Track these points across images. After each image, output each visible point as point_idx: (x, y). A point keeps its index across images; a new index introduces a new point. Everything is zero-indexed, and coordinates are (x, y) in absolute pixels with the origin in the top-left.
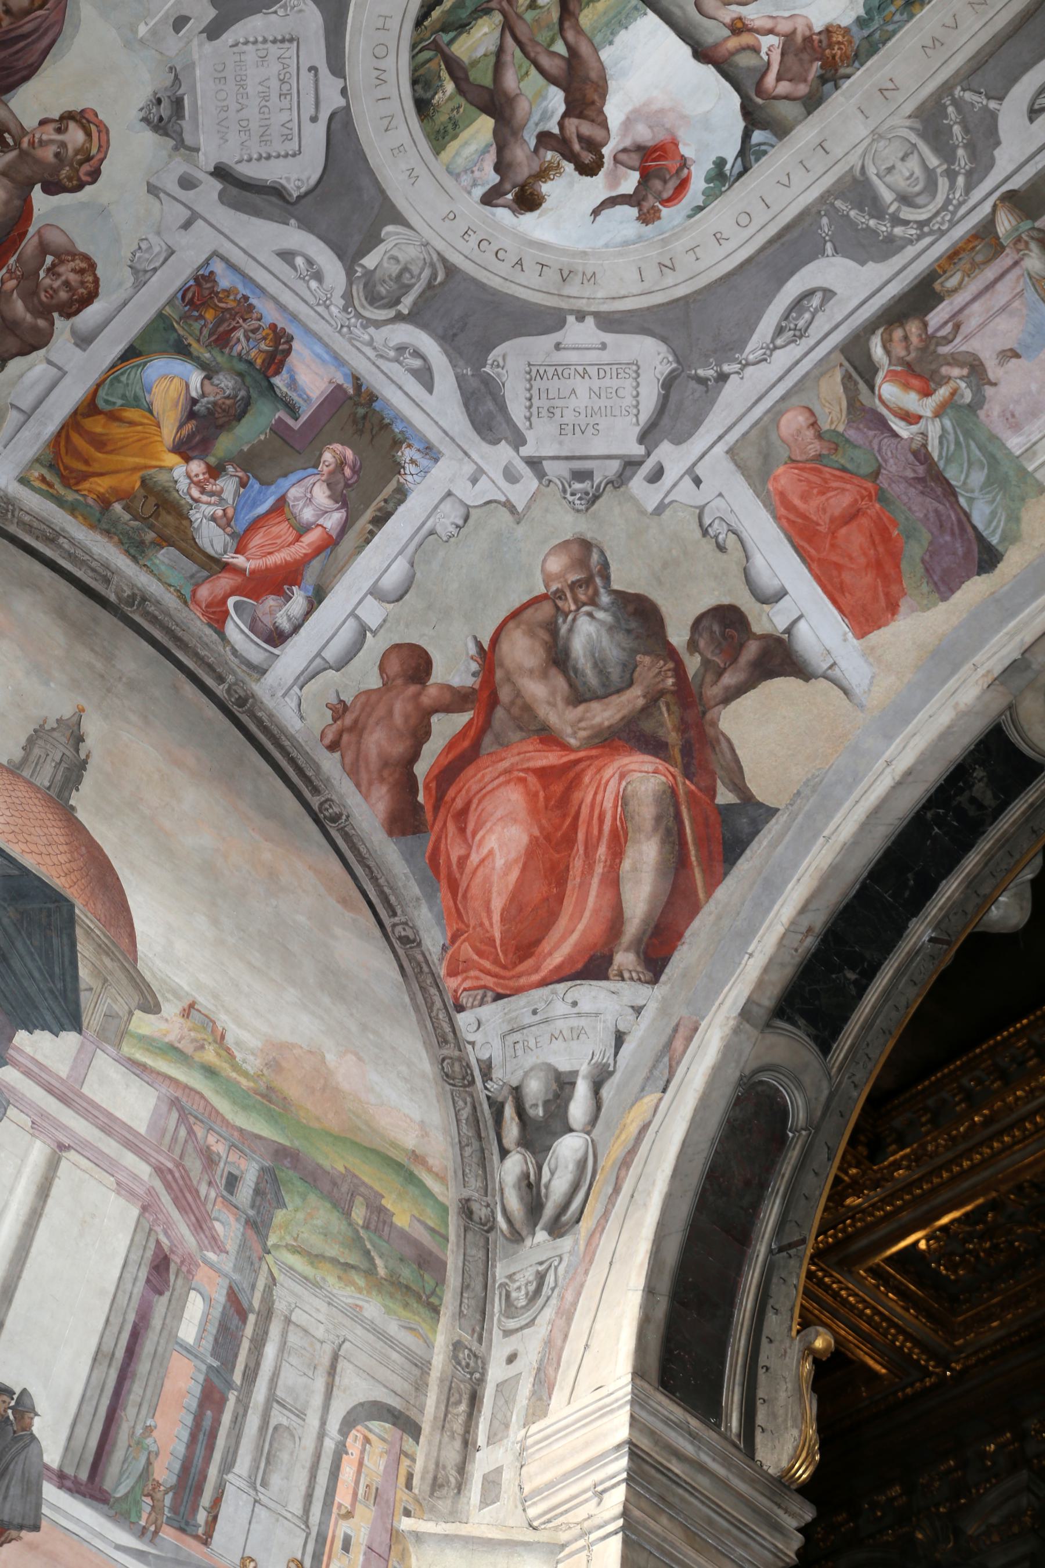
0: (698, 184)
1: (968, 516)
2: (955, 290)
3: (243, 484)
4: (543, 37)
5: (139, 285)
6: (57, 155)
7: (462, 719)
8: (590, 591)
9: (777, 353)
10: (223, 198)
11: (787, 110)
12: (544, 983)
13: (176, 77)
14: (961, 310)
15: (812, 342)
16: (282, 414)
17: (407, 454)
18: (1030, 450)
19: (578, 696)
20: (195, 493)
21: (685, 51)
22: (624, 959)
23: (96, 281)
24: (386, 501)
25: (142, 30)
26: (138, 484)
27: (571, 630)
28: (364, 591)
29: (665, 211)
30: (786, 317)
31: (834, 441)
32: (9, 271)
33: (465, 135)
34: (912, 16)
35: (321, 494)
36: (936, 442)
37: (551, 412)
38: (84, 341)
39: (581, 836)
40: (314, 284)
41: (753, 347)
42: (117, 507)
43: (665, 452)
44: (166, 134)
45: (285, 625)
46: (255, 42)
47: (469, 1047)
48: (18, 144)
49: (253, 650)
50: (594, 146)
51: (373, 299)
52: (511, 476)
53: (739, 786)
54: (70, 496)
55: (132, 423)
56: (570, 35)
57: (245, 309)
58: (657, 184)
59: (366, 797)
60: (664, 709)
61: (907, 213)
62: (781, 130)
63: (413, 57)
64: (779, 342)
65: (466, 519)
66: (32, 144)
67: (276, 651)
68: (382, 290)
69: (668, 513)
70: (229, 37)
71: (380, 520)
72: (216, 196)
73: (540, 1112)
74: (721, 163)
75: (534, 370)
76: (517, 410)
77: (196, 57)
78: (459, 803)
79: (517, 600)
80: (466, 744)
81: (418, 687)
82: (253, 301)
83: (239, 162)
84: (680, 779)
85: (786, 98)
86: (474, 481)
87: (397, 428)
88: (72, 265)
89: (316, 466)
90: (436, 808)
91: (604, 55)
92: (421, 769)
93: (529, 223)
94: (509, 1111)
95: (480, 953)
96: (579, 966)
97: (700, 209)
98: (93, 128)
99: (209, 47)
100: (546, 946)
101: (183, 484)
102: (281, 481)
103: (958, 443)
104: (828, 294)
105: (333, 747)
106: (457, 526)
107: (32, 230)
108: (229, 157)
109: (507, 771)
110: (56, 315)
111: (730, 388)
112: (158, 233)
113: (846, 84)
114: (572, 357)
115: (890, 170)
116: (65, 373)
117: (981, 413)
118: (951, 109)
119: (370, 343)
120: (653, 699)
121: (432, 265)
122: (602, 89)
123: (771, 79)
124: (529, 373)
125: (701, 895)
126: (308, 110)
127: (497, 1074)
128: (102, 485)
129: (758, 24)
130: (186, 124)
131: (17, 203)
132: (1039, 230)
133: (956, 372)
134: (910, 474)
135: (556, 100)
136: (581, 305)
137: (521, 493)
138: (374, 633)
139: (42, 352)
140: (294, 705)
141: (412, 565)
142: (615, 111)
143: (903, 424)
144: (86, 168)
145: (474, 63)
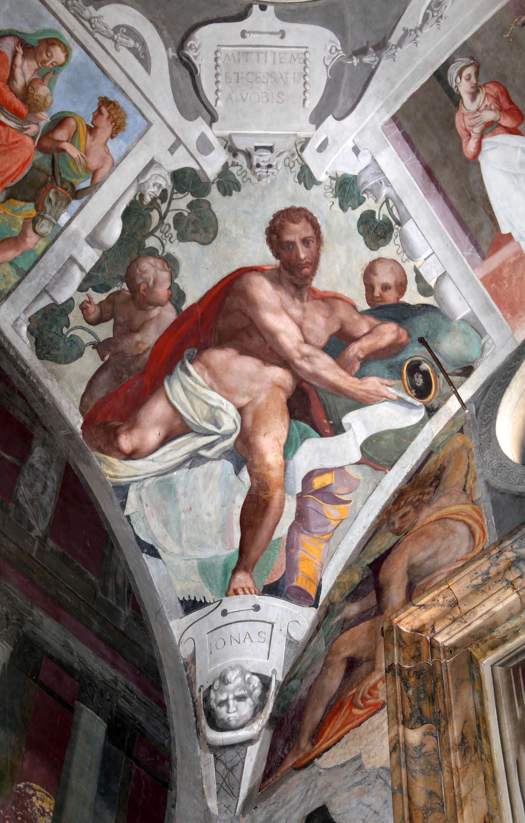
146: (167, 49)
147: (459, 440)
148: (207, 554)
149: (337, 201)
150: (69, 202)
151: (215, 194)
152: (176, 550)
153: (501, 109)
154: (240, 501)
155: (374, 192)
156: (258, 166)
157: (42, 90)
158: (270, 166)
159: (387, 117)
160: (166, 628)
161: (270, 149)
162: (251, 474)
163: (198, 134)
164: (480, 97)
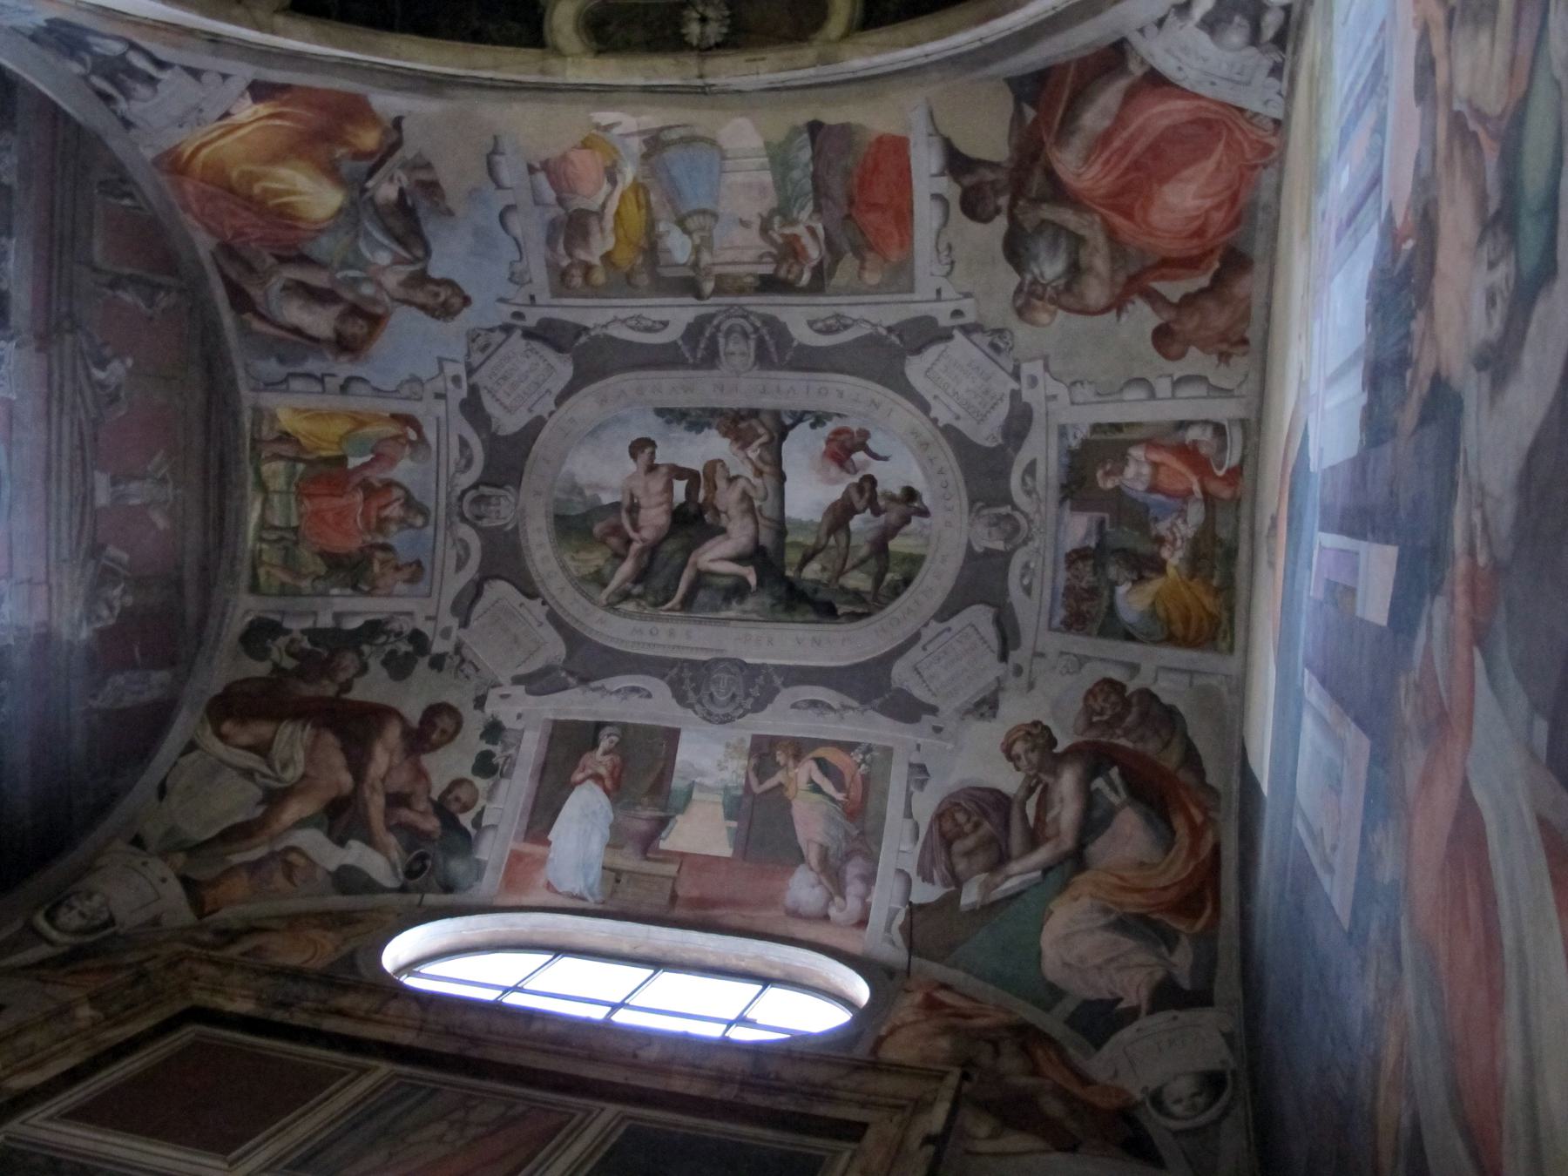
0: (831, 426)
1: (813, 158)
2: (750, 274)
3: (1156, 520)
4: (833, 553)
5: (1088, 658)
6: (1033, 750)
7: (1161, 286)
8: (1034, 287)
9: (855, 316)
10: (1017, 646)
11: (766, 418)
12: (1197, 96)
14: (755, 263)
15: (835, 308)
16: (1108, 528)
17: (1074, 444)
18: (762, 168)
19: (1078, 241)
20: (1179, 543)
21: (787, 485)
22: (1136, 70)
23: (1097, 684)
24: (1105, 433)
25: (950, 746)
26: (1196, 580)
27: (1059, 277)
28: (1159, 402)
29: (855, 429)
30: (837, 331)
31: (858, 252)
32: (1112, 736)
33: (907, 551)
34: (688, 409)
35: (1130, 471)
36: (806, 209)
37: (987, 392)
38: (1134, 668)
39: (1125, 163)
40: (1032, 565)
41: (865, 330)
42: (1215, 582)
43: (944, 321)
45: (1209, 431)
46: (927, 686)
47: (1284, 93)
48: (1036, 776)
49: (1235, 436)
50: (859, 487)
51: (1017, 529)
52: (1034, 381)
53: (1018, 114)
54: (1225, 615)
55: (1166, 610)
56: (823, 542)
57: (1069, 590)
58: (848, 444)
59: (1249, 297)
60: (1034, 191)
61: (749, 329)
62: (776, 414)
63: (887, 605)
64: (849, 322)
65: (1074, 383)
67: (1226, 423)
68: (1008, 528)
69: (965, 290)
70: (932, 701)
71: (1117, 427)
72: (1019, 652)
73: (1237, 19)
74: (813, 426)
75: (979, 418)
76: (1003, 409)
78: (1195, 242)
79: (1078, 322)
80: (1164, 271)
81: (1172, 325)
82: (1061, 590)
83: (993, 651)
84: (1048, 145)
85: (763, 425)
86: (1054, 397)
87: (1066, 460)
89: (1118, 489)
90: (1212, 251)
91: (818, 519)
92: (1204, 281)
93: (919, 484)
94: (1269, 32)
95: (1240, 144)
96: (1166, 89)
97: (839, 415)
98: (1011, 740)
99: (942, 707)
100: (1185, 117)
101: (1179, 554)
102: (1140, 500)
103: (796, 199)
104: (811, 324)
105: (1245, 342)
106: (1082, 383)
107: (1081, 739)
108: (991, 658)
109: (1151, 235)
110: (1127, 694)
111: (891, 320)
112: (1054, 668)
113: (735, 407)
114: (956, 408)
115: (743, 354)
117: (775, 205)
118: (699, 355)
119: (1038, 511)
120: (1038, 201)
121: (979, 510)
122: (833, 507)
123: (764, 439)
124: (982, 420)
125: (1072, 69)
126: (947, 635)
127: (1267, 63)
128: (1208, 601)
129: (750, 466)
130: (987, 693)
132: (695, 271)
133: (775, 236)
134: (830, 203)
135: (856, 523)
136: (929, 425)
137: (1036, 368)
138: (1171, 376)
139: (1154, 689)
140: (1244, 386)
141: (1121, 390)
142: (836, 493)
143: (818, 231)
144: (1035, 731)
145: (868, 573)
146: (478, 571)
150: (346, 586)
153: (612, 774)
155: (506, 747)
156: (462, 671)
157: (393, 528)
159: (551, 717)
163: (447, 624)
164: (607, 758)
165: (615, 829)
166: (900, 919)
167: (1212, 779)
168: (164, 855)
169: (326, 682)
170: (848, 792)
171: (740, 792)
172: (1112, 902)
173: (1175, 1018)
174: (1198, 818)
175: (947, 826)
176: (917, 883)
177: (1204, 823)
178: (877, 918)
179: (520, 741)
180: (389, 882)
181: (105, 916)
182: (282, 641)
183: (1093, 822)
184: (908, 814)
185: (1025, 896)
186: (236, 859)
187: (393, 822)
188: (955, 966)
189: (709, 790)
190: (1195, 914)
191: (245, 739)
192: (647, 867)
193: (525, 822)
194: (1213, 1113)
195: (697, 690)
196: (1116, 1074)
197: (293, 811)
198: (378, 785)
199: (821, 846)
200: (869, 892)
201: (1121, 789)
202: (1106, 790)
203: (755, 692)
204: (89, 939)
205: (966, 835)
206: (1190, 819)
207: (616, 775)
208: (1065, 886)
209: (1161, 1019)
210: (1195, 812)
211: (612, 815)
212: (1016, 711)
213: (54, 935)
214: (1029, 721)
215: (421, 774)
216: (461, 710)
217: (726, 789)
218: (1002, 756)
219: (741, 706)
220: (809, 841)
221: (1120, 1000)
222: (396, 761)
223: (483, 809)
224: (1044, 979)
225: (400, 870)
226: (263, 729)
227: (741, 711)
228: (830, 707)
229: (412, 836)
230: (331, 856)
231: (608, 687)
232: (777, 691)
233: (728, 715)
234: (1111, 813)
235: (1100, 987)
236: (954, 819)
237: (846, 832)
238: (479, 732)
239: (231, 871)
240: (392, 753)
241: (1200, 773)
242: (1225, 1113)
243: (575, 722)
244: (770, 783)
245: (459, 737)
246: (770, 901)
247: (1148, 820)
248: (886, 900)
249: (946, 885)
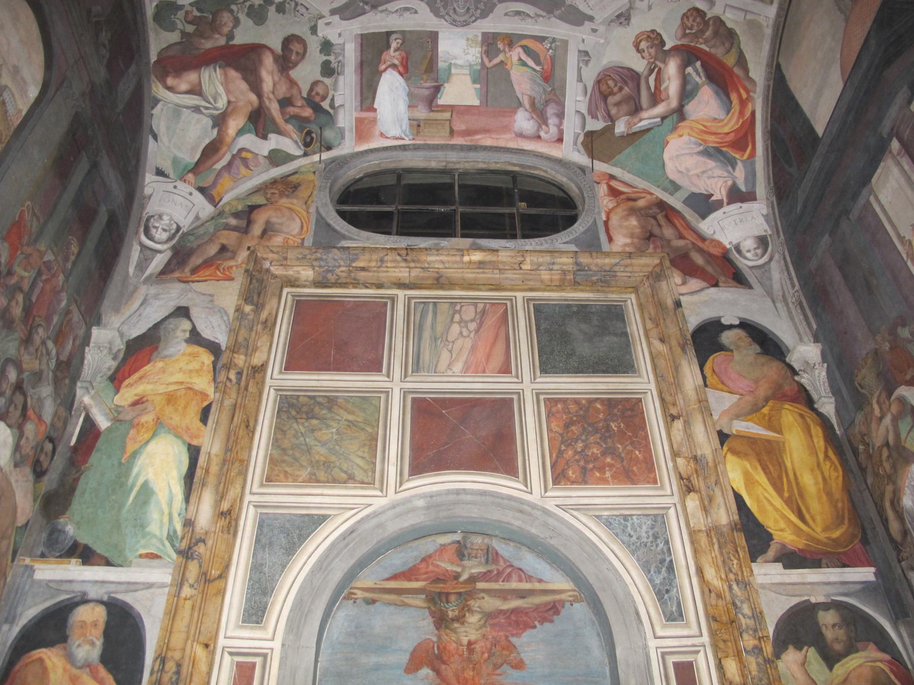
6: (652, 48)
13: (611, 22)
23: (689, 10)
25: (602, 41)
44: (629, 15)
48: (653, 63)
66: (651, 58)
70: (589, 12)
77: (602, 20)
88: (687, 22)
99: (597, 17)
107: (679, 43)
110: (706, 19)
116: (726, 5)
130: (623, 10)
131: (672, 53)
139: (723, 18)
144: (652, 36)
147: (311, 177)
148: (180, 155)
149: (320, 47)
151: (272, 9)
152: (167, 144)
153: (402, 63)
154: (207, 141)
155: (337, 55)
158: (302, 15)
159: (359, 32)
160: (144, 176)
161: (307, 9)
162: (218, 133)
164: (397, 53)
165: (410, 95)
166: (581, 139)
167: (752, 74)
168: (182, 179)
169: (217, 36)
170: (543, 66)
171: (479, 67)
172: (702, 140)
173: (741, 207)
174: (744, 96)
175: (603, 88)
176: (588, 119)
177: (747, 98)
178: (568, 138)
179: (344, 50)
180: (298, 152)
181: (175, 226)
182: (181, 14)
183: (687, 93)
184: (580, 79)
185: (652, 131)
186: (218, 166)
187: (288, 117)
188: (615, 165)
189: (462, 67)
190: (743, 149)
191: (184, 87)
192: (433, 115)
193: (359, 99)
194: (766, 258)
195: (445, 7)
196: (714, 232)
197: (234, 125)
198: (271, 96)
199: (530, 97)
200: (561, 123)
201: (702, 74)
202: (694, 74)
203: (481, 6)
204: (174, 242)
205: (614, 94)
206: (740, 96)
207: (404, 63)
208: (675, 128)
209: (734, 207)
210: (742, 91)
211: (407, 88)
212: (641, 23)
213: (158, 247)
214: (649, 30)
215: (293, 83)
216: (304, 38)
217: (471, 66)
218: (634, 50)
219: (473, 15)
220: (523, 94)
221: (713, 195)
222: (276, 78)
223: (333, 96)
224: (668, 178)
225: (300, 144)
226: (192, 77)
227: (474, 18)
228: (528, 15)
229: (300, 122)
230: (264, 147)
231: (390, 9)
232: (494, 5)
233: (465, 21)
234: (697, 88)
235: (701, 187)
236: (607, 84)
237: (544, 89)
238: (318, 50)
239: (219, 174)
240: (272, 73)
241: (746, 71)
242: (771, 259)
243: (374, 33)
244: (496, 61)
245: (307, 54)
246: (506, 129)
247: (717, 93)
248: (572, 127)
249: (605, 121)
